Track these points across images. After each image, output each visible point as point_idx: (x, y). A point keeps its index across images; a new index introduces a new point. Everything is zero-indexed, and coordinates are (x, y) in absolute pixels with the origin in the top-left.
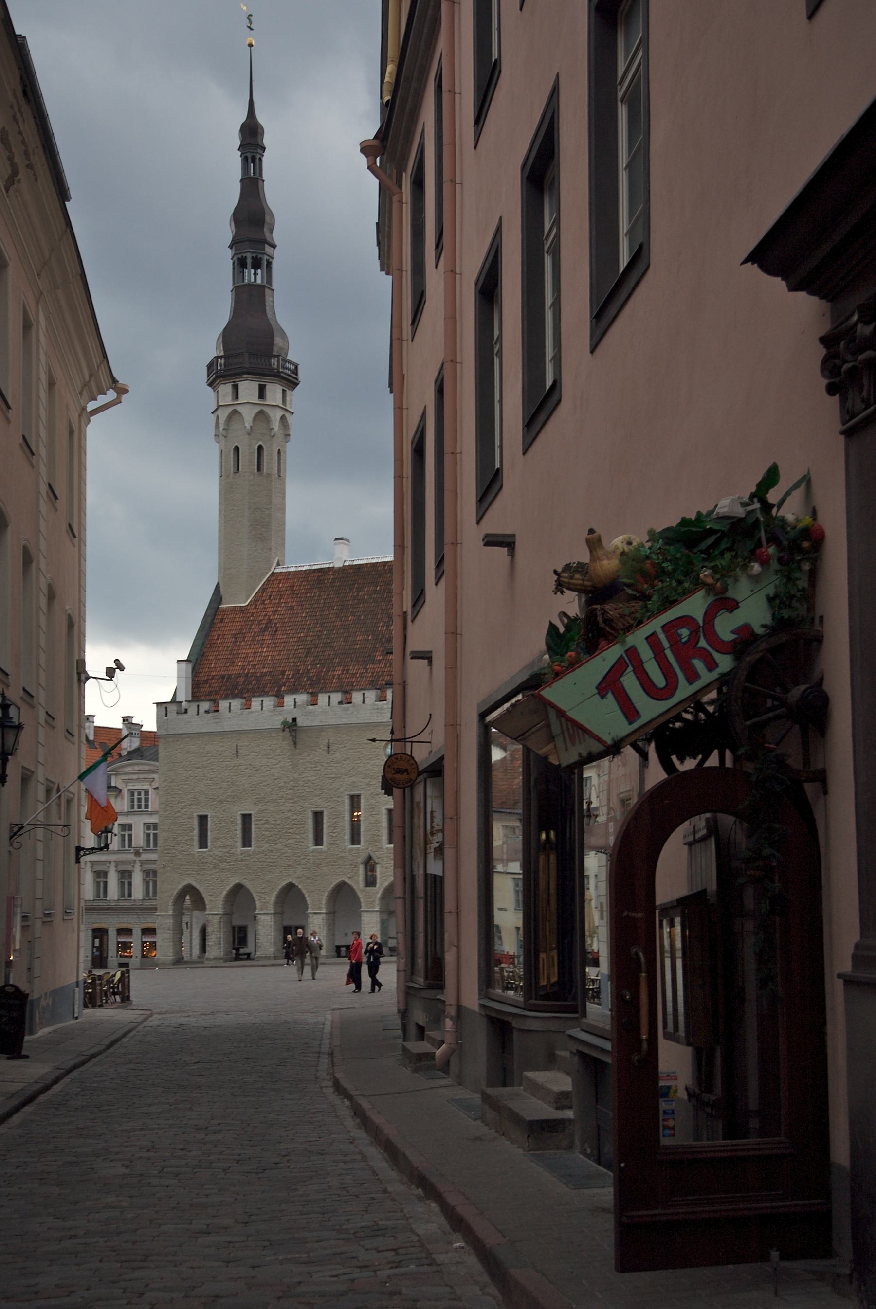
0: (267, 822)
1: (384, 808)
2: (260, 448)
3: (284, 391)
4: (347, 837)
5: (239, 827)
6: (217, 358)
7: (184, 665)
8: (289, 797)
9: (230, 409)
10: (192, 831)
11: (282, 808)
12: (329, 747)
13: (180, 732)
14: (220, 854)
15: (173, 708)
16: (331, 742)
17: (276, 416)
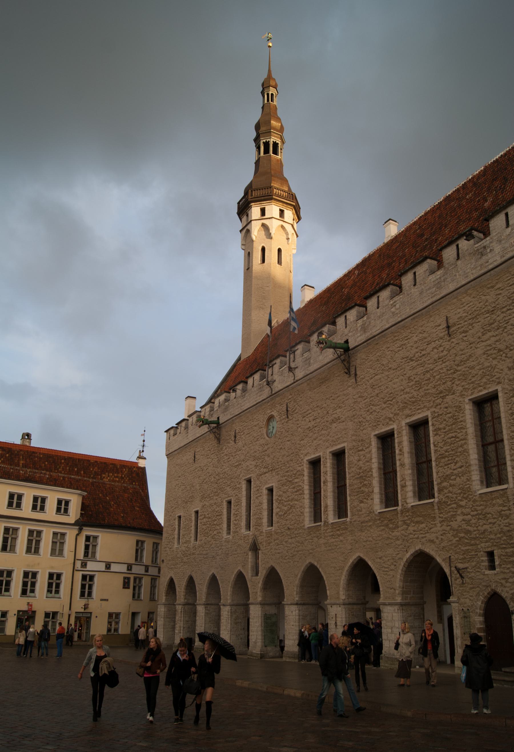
0: (204, 518)
1: (264, 489)
2: (263, 249)
3: (282, 212)
4: (243, 523)
5: (193, 523)
6: (239, 203)
7: (189, 400)
8: (215, 490)
9: (245, 231)
10: (175, 530)
11: (212, 502)
12: (235, 437)
13: (173, 450)
14: (184, 549)
15: (172, 432)
16: (237, 431)
17: (274, 225)
